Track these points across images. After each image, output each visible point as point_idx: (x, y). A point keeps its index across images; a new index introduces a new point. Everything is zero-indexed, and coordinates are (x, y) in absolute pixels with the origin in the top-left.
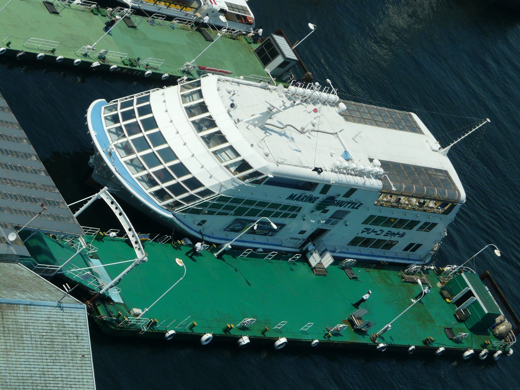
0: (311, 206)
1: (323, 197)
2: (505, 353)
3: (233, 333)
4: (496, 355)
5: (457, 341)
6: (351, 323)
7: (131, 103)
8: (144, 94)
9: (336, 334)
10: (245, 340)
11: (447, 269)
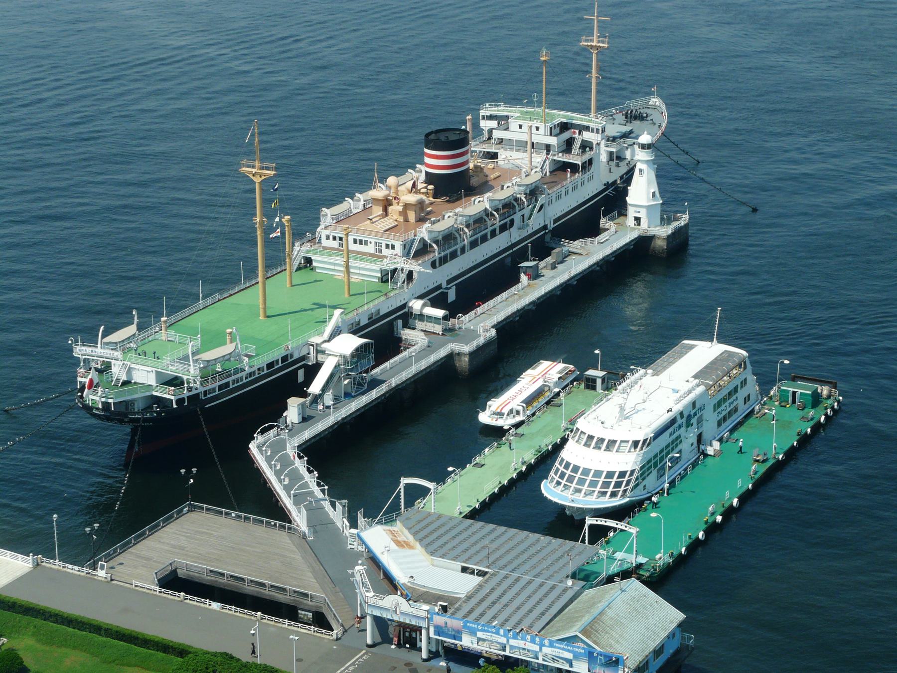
0: (683, 429)
1: (684, 420)
2: (839, 402)
3: (710, 521)
4: (836, 407)
5: (812, 419)
6: (757, 461)
7: (558, 469)
8: (559, 459)
9: (755, 473)
10: (719, 519)
11: (772, 393)
